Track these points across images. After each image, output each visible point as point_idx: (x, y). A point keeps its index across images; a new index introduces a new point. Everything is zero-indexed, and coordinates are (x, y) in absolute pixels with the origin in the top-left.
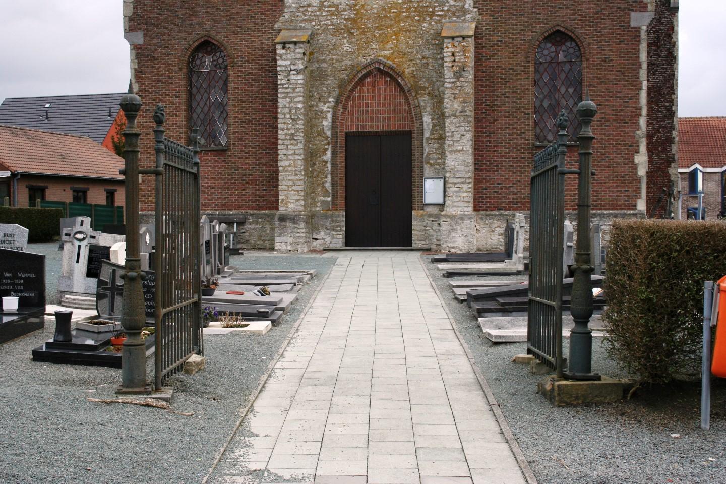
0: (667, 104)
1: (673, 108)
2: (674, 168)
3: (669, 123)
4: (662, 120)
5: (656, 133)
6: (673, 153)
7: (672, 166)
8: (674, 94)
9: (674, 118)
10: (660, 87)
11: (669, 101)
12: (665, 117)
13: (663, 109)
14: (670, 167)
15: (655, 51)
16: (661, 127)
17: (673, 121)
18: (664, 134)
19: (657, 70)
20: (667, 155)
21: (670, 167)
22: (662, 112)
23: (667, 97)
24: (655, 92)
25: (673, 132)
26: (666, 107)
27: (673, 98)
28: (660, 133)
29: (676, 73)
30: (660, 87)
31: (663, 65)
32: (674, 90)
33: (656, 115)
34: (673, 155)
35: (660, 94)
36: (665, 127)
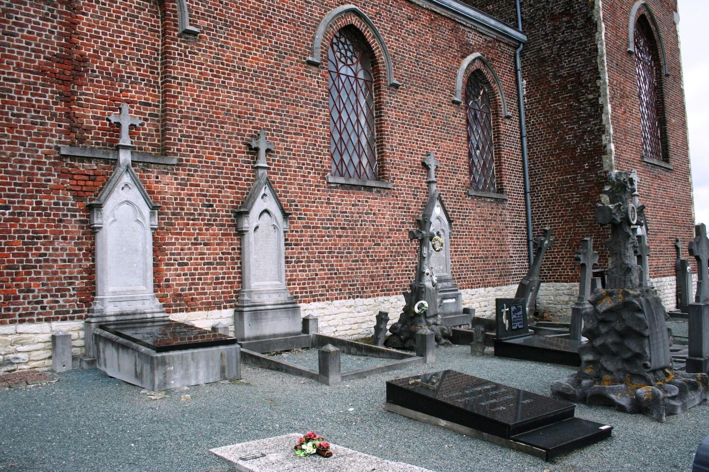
0: (591, 97)
1: (601, 101)
3: (595, 125)
4: (586, 122)
5: (578, 143)
6: (605, 170)
8: (599, 78)
9: (603, 115)
10: (579, 74)
11: (594, 90)
12: (590, 116)
13: (585, 104)
15: (568, 22)
16: (584, 133)
17: (601, 120)
18: (590, 143)
19: (573, 49)
20: (596, 174)
22: (584, 109)
23: (589, 85)
24: (572, 82)
25: (604, 137)
26: (590, 100)
27: (598, 85)
28: (585, 141)
29: (599, 46)
30: (579, 74)
31: (581, 39)
32: (599, 73)
33: (577, 115)
34: (606, 172)
35: (580, 84)
36: (591, 132)
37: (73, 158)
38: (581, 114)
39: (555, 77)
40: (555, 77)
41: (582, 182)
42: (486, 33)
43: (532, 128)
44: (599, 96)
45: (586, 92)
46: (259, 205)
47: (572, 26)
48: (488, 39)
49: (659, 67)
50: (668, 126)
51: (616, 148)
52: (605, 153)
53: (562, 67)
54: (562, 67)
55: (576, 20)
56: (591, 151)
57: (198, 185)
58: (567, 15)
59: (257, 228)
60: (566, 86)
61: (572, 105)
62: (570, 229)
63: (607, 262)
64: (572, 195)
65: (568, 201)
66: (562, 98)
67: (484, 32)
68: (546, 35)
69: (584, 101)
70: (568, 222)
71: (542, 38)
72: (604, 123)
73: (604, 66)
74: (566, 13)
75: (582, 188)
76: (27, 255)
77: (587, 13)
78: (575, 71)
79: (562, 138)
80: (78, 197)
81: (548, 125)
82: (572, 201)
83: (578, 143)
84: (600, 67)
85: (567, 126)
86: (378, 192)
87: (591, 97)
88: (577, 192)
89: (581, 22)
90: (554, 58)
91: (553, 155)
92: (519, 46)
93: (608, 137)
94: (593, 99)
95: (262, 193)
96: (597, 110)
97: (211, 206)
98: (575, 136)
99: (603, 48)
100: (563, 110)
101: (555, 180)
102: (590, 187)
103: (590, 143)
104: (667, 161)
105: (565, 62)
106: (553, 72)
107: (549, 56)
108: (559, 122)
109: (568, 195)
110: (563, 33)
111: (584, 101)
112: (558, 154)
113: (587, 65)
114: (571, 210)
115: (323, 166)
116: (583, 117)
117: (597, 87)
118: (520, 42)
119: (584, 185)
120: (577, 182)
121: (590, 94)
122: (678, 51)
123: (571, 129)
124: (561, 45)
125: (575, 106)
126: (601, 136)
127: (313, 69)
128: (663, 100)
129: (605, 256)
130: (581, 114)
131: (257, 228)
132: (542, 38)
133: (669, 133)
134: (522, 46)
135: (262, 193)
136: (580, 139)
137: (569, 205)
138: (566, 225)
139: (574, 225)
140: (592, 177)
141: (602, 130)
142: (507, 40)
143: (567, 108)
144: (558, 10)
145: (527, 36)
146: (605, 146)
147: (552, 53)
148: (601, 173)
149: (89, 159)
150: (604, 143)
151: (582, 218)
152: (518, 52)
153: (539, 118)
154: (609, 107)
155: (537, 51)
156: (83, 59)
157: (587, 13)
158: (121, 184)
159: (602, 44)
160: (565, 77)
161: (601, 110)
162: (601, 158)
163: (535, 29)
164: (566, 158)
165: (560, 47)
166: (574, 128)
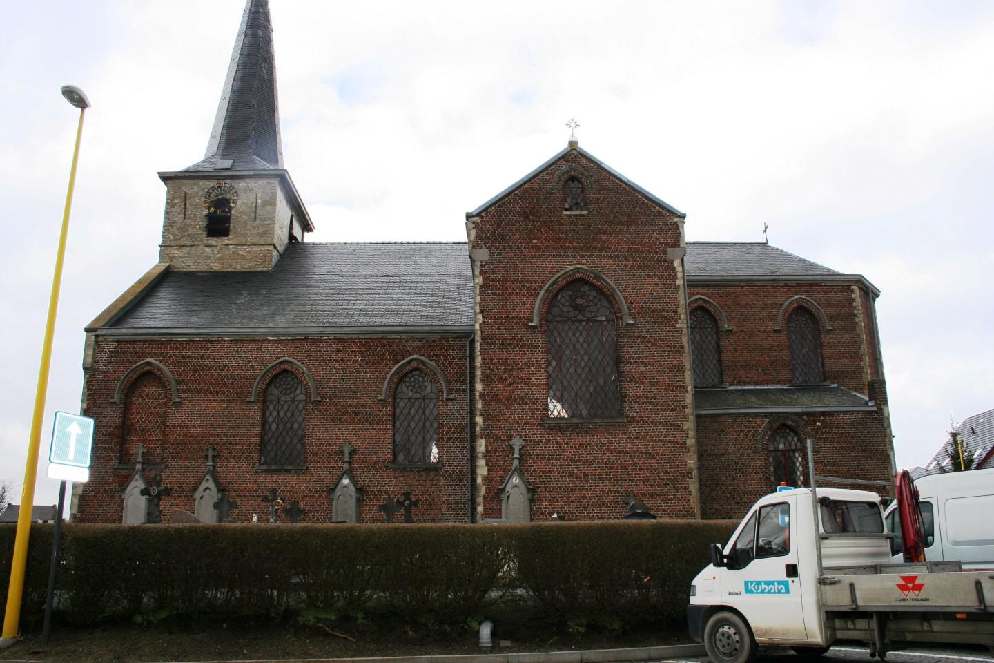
37: (120, 469)
46: (204, 485)
48: (431, 340)
57: (175, 477)
59: (202, 497)
76: (98, 510)
80: (120, 486)
86: (296, 472)
95: (206, 478)
97: (182, 486)
115: (253, 460)
127: (253, 404)
131: (202, 497)
135: (206, 478)
149: (126, 469)
156: (132, 425)
158: (135, 479)
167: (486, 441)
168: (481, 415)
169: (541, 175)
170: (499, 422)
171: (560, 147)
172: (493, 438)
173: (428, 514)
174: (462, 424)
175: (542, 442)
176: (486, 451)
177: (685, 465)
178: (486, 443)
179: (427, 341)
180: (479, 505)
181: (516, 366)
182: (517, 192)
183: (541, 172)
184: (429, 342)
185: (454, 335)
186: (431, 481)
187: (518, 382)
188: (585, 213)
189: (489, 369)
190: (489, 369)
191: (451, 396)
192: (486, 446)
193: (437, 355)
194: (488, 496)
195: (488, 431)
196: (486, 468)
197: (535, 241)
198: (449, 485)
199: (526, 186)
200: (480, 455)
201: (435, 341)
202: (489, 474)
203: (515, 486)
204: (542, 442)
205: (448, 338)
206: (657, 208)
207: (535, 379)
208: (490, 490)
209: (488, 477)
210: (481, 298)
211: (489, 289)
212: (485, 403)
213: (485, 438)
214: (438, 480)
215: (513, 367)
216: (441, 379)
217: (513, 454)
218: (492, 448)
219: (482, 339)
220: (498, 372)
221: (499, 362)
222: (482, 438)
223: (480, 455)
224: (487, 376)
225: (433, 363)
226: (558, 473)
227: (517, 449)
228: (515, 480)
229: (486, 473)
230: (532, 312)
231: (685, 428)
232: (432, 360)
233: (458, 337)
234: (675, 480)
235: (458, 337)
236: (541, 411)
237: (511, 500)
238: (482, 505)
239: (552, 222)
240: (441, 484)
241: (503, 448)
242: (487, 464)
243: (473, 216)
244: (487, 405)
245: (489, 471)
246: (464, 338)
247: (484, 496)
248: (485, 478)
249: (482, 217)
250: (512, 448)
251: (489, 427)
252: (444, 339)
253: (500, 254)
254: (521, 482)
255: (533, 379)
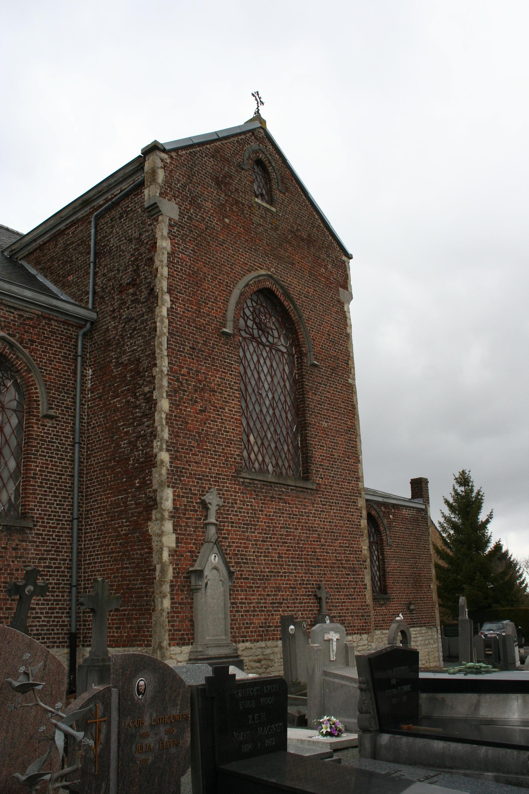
0: (147, 389)
1: (155, 394)
2: (157, 520)
3: (148, 426)
6: (154, 488)
7: (154, 517)
8: (155, 365)
12: (145, 415)
13: (141, 401)
14: (150, 519)
15: (134, 294)
17: (154, 420)
19: (135, 329)
21: (150, 519)
23: (147, 373)
24: (132, 370)
26: (145, 394)
27: (154, 374)
29: (158, 324)
31: (143, 315)
32: (155, 359)
34: (155, 491)
35: (138, 373)
38: (136, 413)
39: (118, 365)
40: (118, 365)
41: (132, 504)
42: (21, 308)
43: (92, 432)
44: (154, 389)
45: (143, 384)
47: (137, 299)
48: (27, 315)
49: (301, 355)
50: (311, 431)
51: (173, 459)
52: (154, 465)
53: (124, 352)
54: (124, 352)
55: (141, 292)
56: (142, 463)
58: (134, 285)
60: (126, 376)
61: (129, 401)
62: (118, 569)
63: (151, 618)
64: (122, 522)
65: (118, 532)
66: (122, 392)
67: (16, 306)
68: (113, 311)
69: (140, 395)
70: (117, 560)
71: (110, 315)
72: (156, 424)
73: (161, 350)
74: (133, 284)
75: (132, 513)
77: (150, 283)
78: (135, 357)
79: (118, 446)
81: (106, 427)
82: (122, 531)
83: (132, 450)
84: (157, 351)
85: (123, 429)
87: (147, 389)
88: (127, 519)
89: (145, 293)
90: (118, 340)
91: (108, 468)
92: (85, 325)
93: (159, 444)
94: (149, 392)
96: (150, 409)
98: (130, 443)
99: (163, 327)
100: (121, 407)
101: (108, 502)
102: (139, 513)
103: (143, 451)
104: (306, 479)
105: (127, 346)
106: (116, 358)
107: (114, 338)
108: (117, 424)
109: (118, 523)
110: (128, 308)
111: (140, 395)
112: (113, 466)
113: (146, 349)
114: (120, 544)
116: (137, 417)
117: (153, 376)
118: (86, 321)
119: (134, 508)
120: (128, 505)
121: (146, 386)
122: (348, 337)
123: (127, 433)
124: (126, 323)
125: (132, 402)
126: (152, 441)
128: (303, 397)
129: (149, 609)
130: (136, 413)
132: (110, 315)
133: (312, 441)
134: (88, 325)
136: (133, 445)
137: (119, 535)
138: (115, 565)
139: (122, 564)
140: (141, 498)
141: (154, 435)
142: (62, 318)
143: (124, 406)
144: (126, 280)
145: (97, 313)
146: (156, 455)
147: (116, 334)
148: (150, 492)
150: (155, 451)
151: (130, 555)
152: (81, 332)
153: (99, 418)
154: (164, 404)
155: (105, 332)
157: (150, 283)
159: (162, 322)
160: (126, 365)
161: (155, 407)
162: (151, 472)
163: (106, 304)
164: (120, 472)
165: (124, 327)
166: (128, 431)
167: (174, 491)
168: (168, 450)
169: (232, 139)
170: (189, 465)
171: (233, 116)
172: (182, 488)
173: (7, 609)
174: (63, 459)
175: (236, 503)
176: (174, 508)
177: (361, 551)
178: (174, 495)
179: (19, 315)
180: (164, 597)
181: (208, 386)
182: (208, 146)
183: (233, 136)
184: (22, 316)
185: (62, 318)
186: (14, 549)
187: (210, 409)
188: (274, 209)
189: (178, 380)
190: (178, 380)
191: (52, 412)
192: (174, 500)
193: (32, 341)
194: (177, 582)
195: (176, 476)
196: (174, 536)
197: (227, 220)
198: (40, 559)
199: (218, 144)
200: (166, 514)
201: (32, 319)
202: (177, 547)
203: (216, 568)
204: (236, 503)
205: (50, 319)
206: (331, 238)
207: (229, 410)
208: (178, 573)
209: (176, 551)
210: (169, 272)
211: (178, 262)
212: (173, 431)
213: (173, 487)
214: (25, 549)
215: (204, 385)
216: (36, 382)
217: (206, 517)
218: (180, 505)
219: (169, 333)
220: (188, 388)
221: (189, 373)
222: (168, 486)
223: (166, 514)
224: (176, 391)
225: (26, 351)
226: (254, 552)
227: (213, 509)
228: (214, 559)
229: (174, 545)
230: (224, 314)
231: (359, 505)
232: (25, 347)
233: (64, 323)
234: (353, 570)
235: (64, 323)
236: (235, 459)
237: (209, 590)
238: (169, 596)
239: (243, 205)
240: (30, 556)
241: (194, 506)
242: (175, 530)
243: (164, 151)
244: (175, 436)
245: (178, 541)
246: (73, 326)
247: (172, 581)
248: (173, 553)
249: (171, 157)
250: (205, 506)
251: (177, 471)
252: (44, 318)
253: (190, 218)
254: (221, 562)
255: (227, 410)
